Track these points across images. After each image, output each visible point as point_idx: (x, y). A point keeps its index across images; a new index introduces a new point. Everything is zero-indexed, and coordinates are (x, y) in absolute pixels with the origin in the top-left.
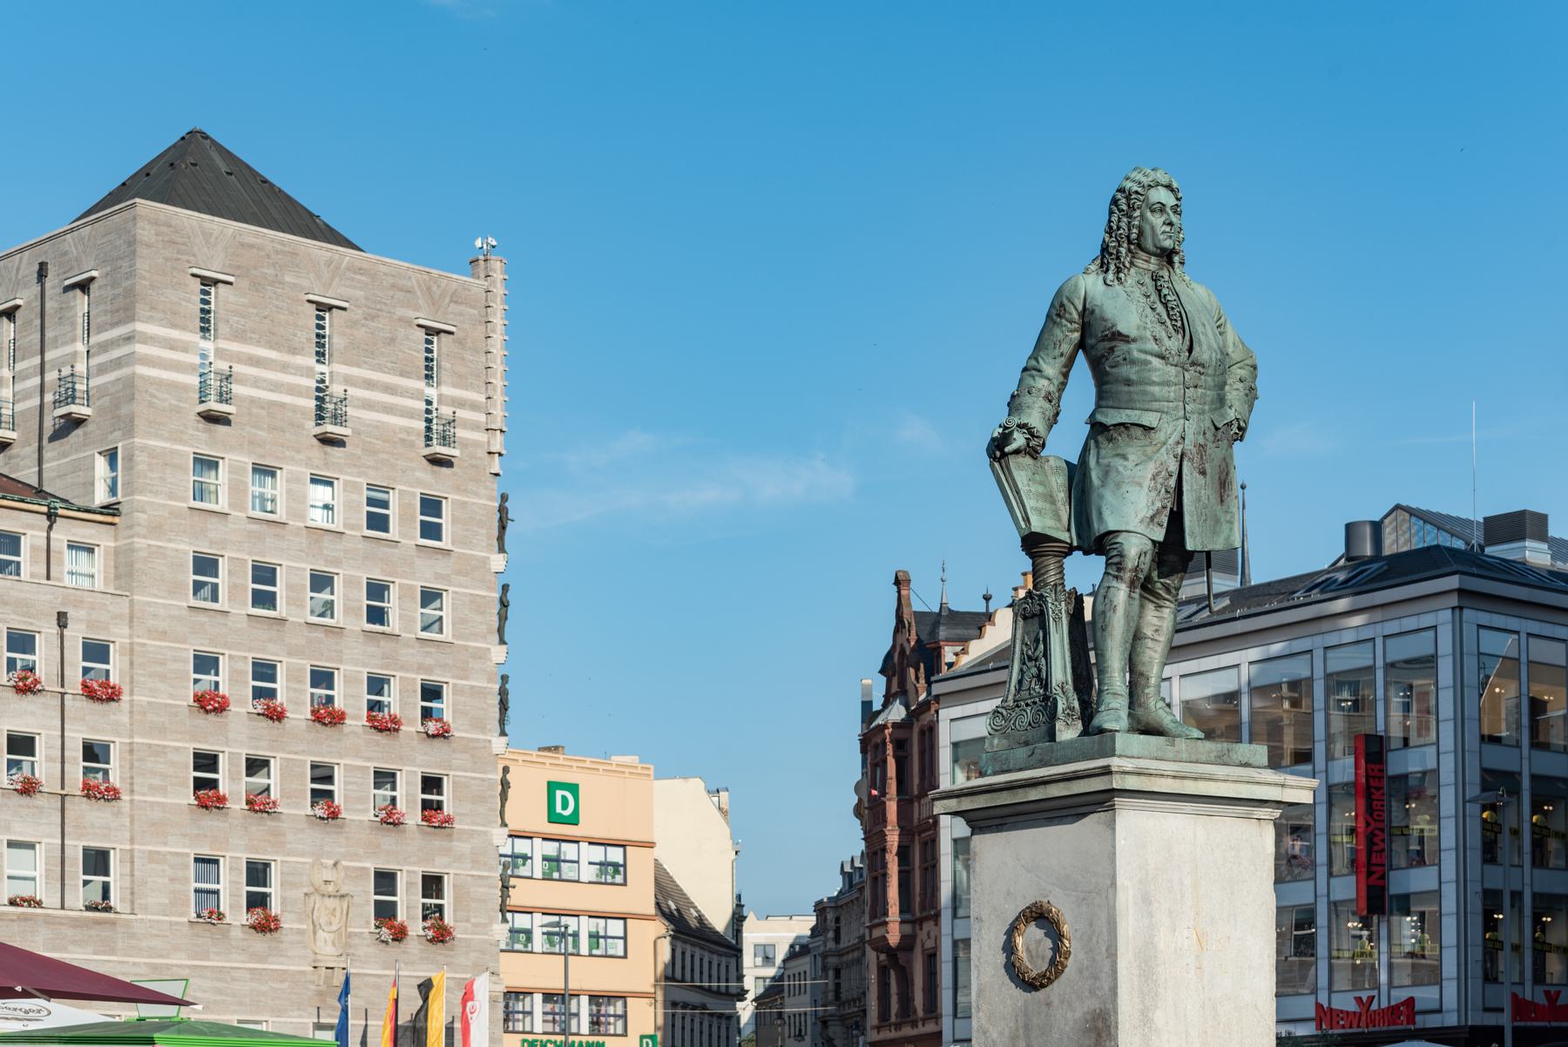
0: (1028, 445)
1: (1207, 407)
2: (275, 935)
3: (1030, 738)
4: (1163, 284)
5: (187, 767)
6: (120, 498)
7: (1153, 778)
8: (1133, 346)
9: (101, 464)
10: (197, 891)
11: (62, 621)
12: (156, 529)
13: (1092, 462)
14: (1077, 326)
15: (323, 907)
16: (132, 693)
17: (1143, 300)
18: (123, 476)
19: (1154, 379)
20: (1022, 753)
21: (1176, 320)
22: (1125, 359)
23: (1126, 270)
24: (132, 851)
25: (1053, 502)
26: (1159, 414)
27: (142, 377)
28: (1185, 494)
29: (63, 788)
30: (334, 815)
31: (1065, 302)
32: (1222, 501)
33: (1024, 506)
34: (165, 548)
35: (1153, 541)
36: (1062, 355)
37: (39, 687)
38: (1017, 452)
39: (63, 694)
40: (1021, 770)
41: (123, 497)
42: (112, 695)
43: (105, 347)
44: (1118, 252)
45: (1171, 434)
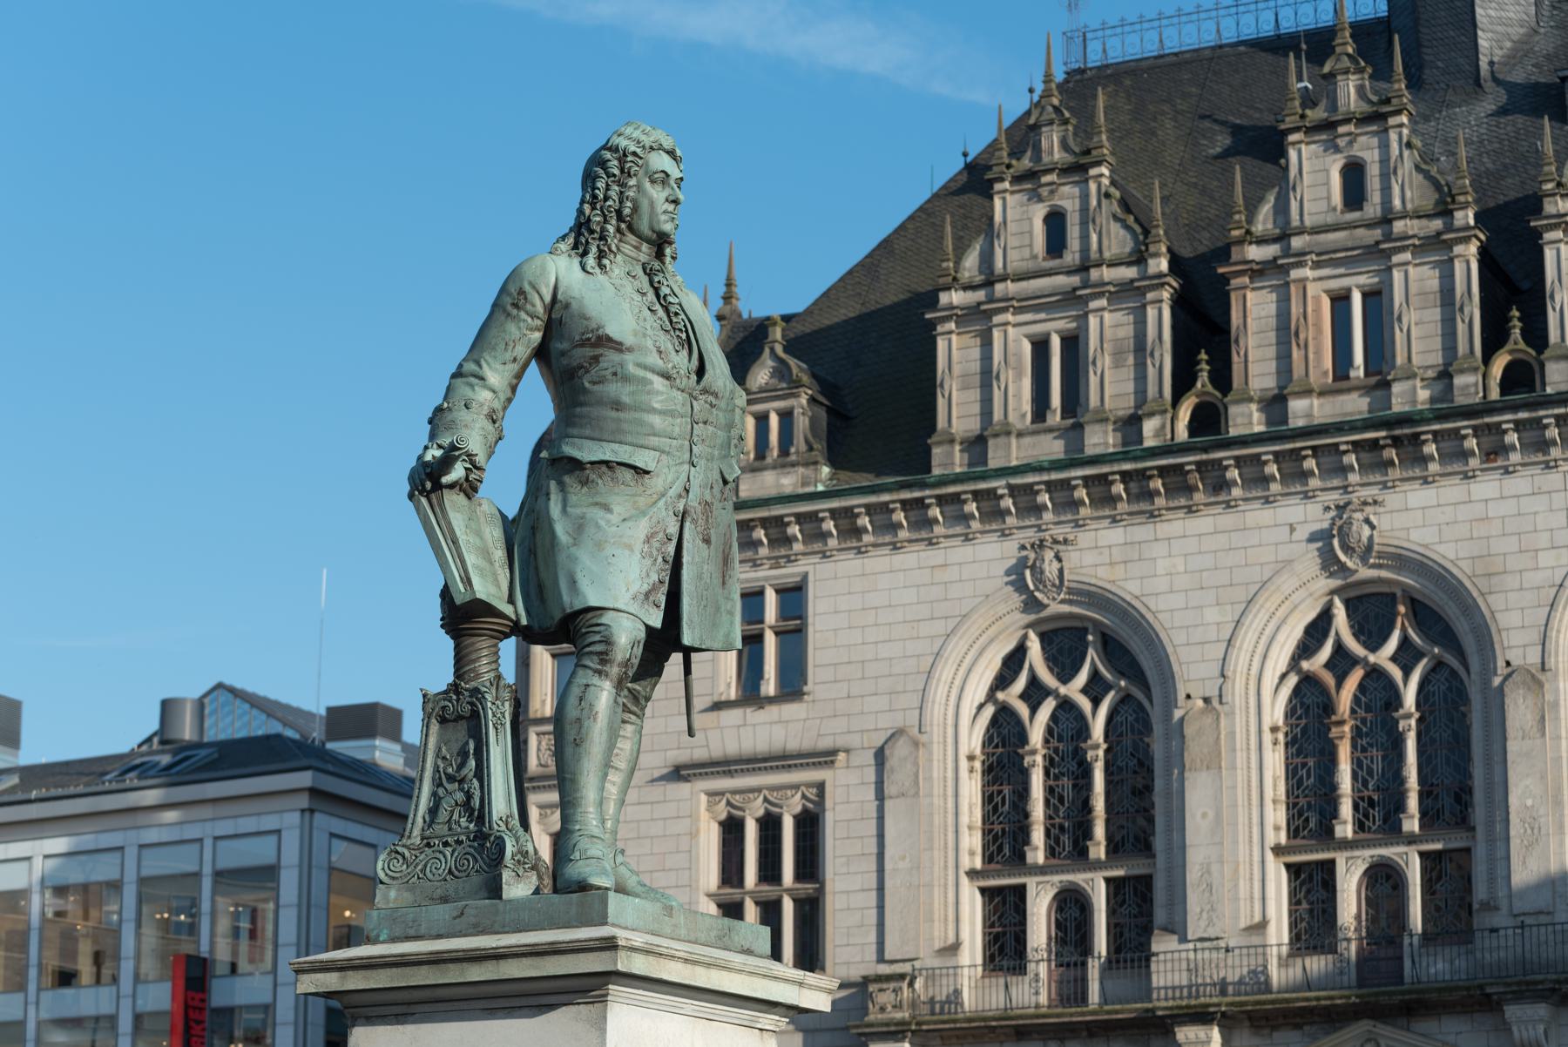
0: (467, 479)
1: (716, 453)
3: (451, 892)
4: (662, 280)
8: (628, 357)
13: (555, 509)
14: (539, 322)
17: (638, 297)
19: (657, 406)
20: (443, 912)
21: (680, 330)
22: (615, 374)
23: (612, 256)
25: (491, 563)
26: (658, 454)
28: (685, 567)
31: (527, 288)
32: (724, 583)
33: (463, 562)
35: (647, 626)
36: (515, 360)
38: (451, 486)
40: (439, 936)
44: (603, 230)
45: (673, 483)
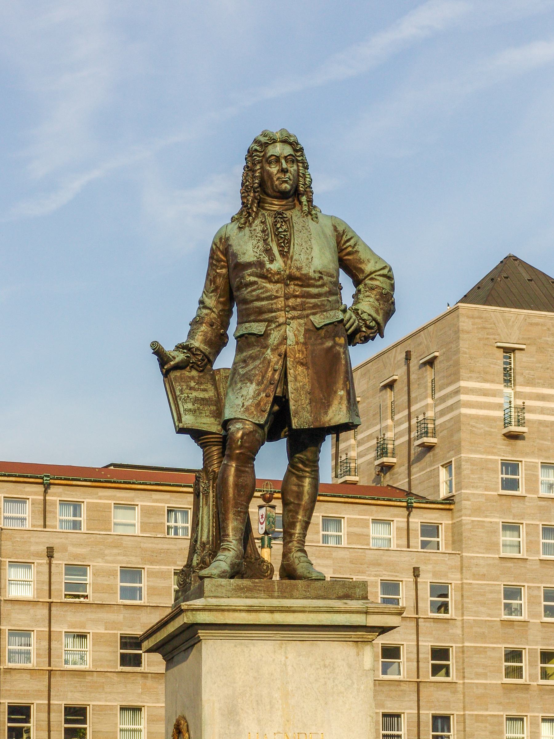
5: (500, 660)
6: (454, 493)
7: (226, 613)
9: (443, 474)
11: (416, 572)
12: (477, 510)
18: (455, 479)
24: (464, 715)
27: (465, 415)
29: (418, 677)
34: (484, 521)
39: (417, 619)
41: (456, 491)
43: (443, 399)
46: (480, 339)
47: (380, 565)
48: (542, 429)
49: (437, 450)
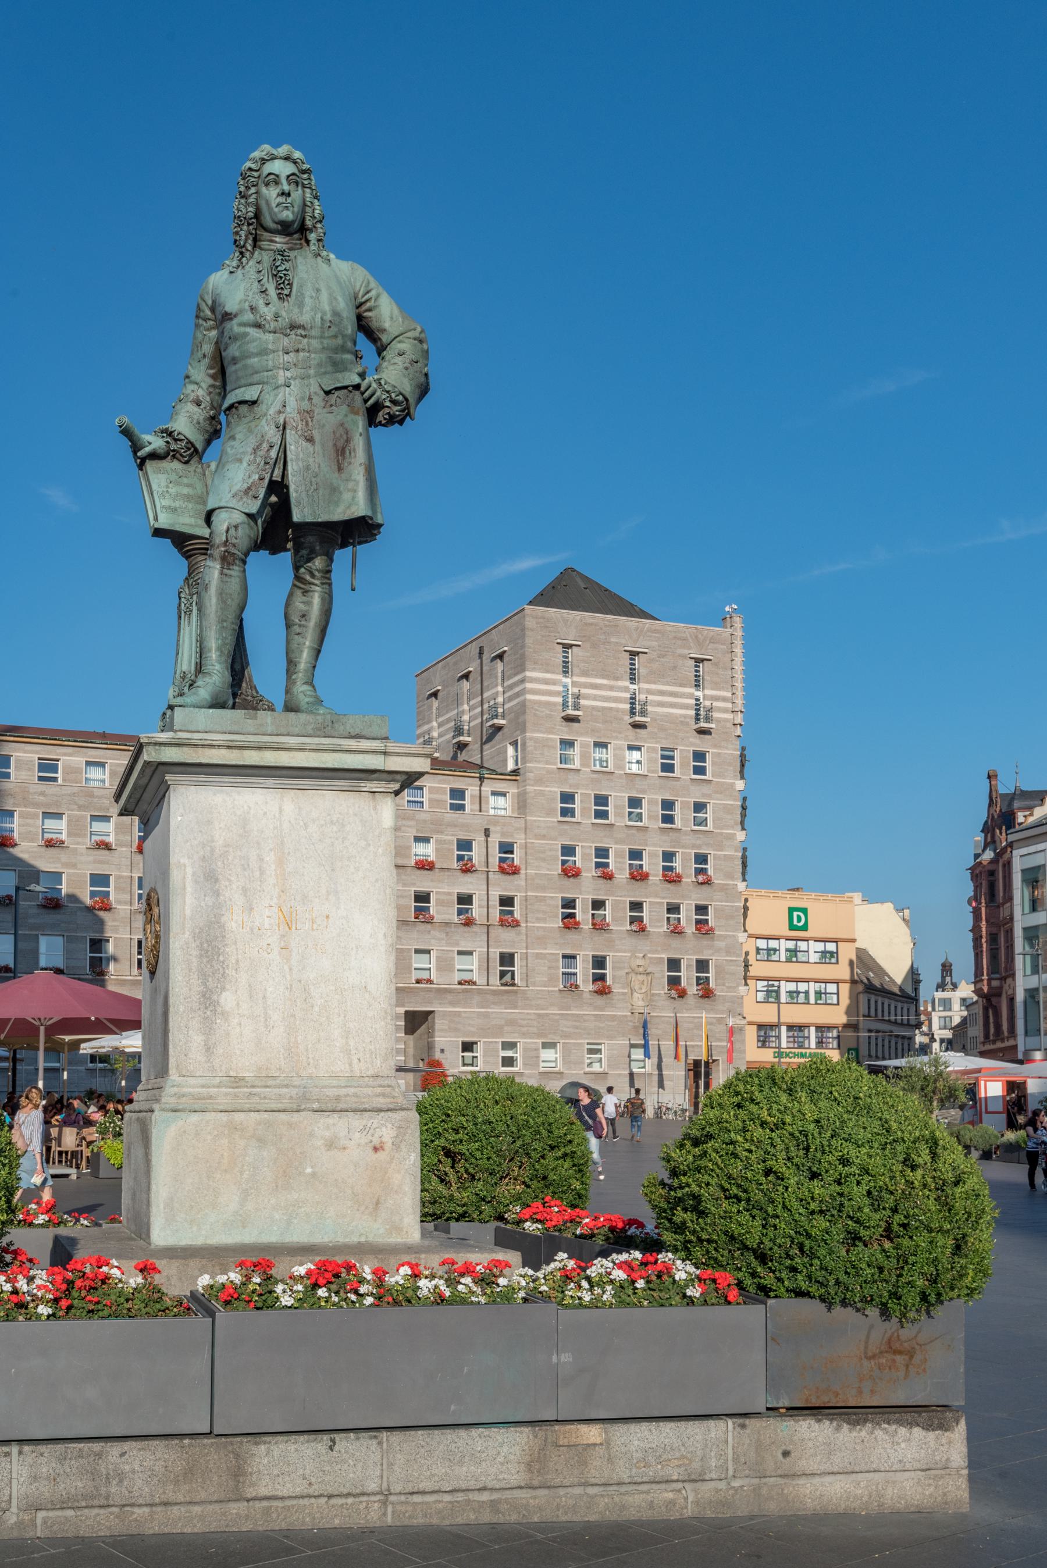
2: (609, 996)
5: (557, 907)
6: (520, 766)
9: (510, 750)
10: (564, 974)
11: (487, 833)
12: (539, 781)
15: (636, 980)
16: (526, 869)
24: (527, 953)
27: (530, 700)
30: (643, 929)
32: (340, 469)
37: (474, 869)
42: (515, 871)
43: (511, 687)
46: (543, 636)
47: (455, 826)
48: (595, 713)
49: (505, 730)
